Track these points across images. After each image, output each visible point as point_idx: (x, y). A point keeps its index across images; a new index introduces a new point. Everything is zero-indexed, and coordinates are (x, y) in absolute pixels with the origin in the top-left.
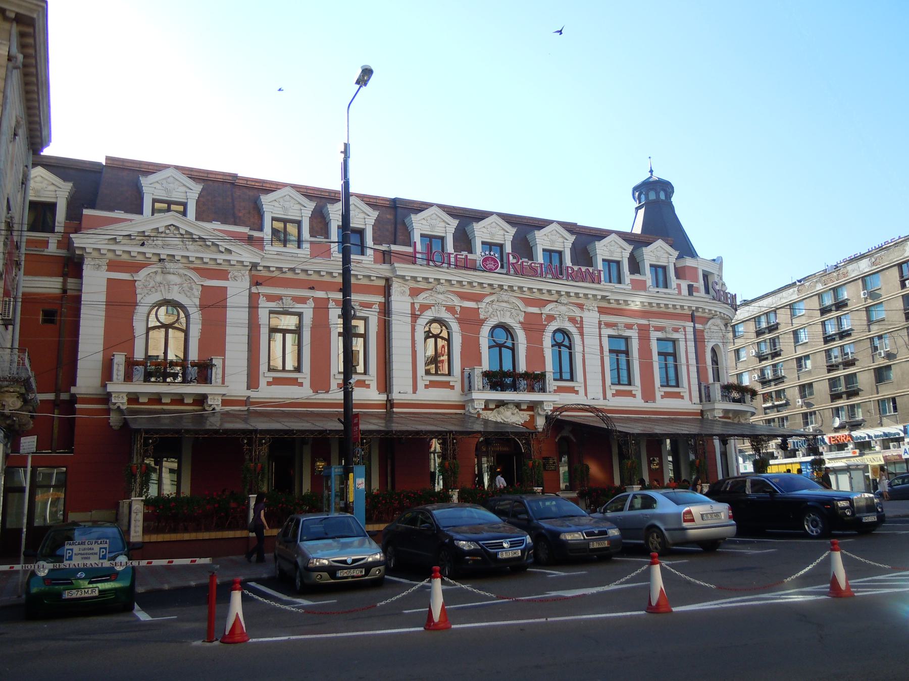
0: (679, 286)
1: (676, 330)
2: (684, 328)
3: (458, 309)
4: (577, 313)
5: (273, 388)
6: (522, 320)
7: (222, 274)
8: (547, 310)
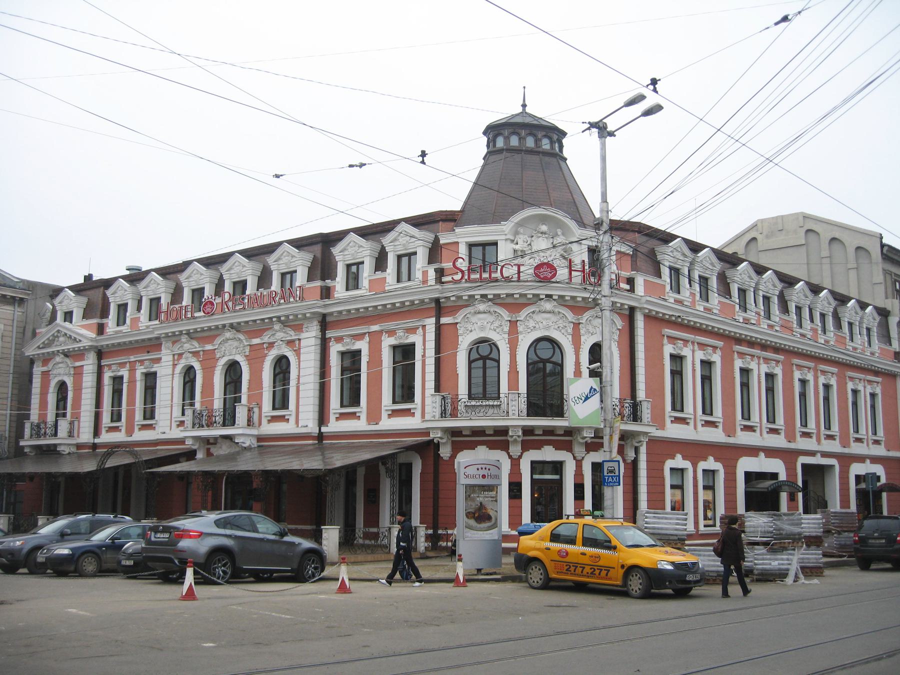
0: (425, 273)
1: (413, 330)
2: (424, 326)
3: (201, 353)
4: (292, 335)
5: (143, 432)
6: (247, 354)
7: (79, 354)
8: (266, 338)
